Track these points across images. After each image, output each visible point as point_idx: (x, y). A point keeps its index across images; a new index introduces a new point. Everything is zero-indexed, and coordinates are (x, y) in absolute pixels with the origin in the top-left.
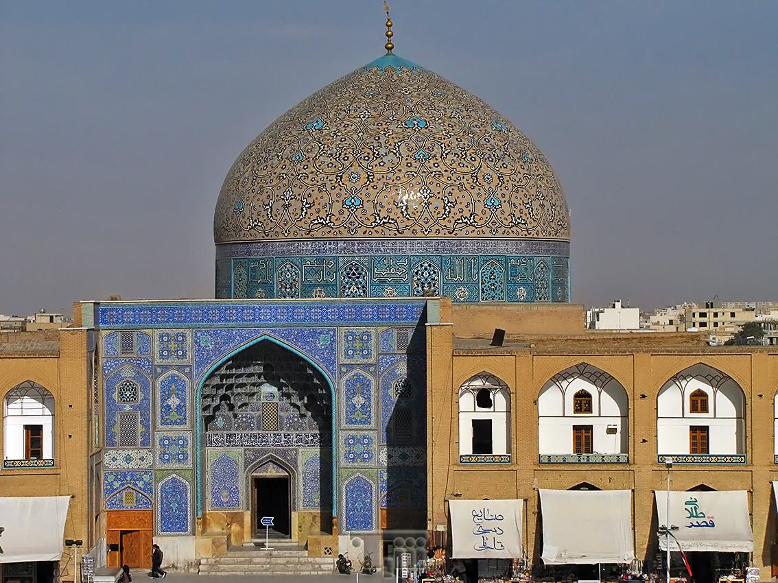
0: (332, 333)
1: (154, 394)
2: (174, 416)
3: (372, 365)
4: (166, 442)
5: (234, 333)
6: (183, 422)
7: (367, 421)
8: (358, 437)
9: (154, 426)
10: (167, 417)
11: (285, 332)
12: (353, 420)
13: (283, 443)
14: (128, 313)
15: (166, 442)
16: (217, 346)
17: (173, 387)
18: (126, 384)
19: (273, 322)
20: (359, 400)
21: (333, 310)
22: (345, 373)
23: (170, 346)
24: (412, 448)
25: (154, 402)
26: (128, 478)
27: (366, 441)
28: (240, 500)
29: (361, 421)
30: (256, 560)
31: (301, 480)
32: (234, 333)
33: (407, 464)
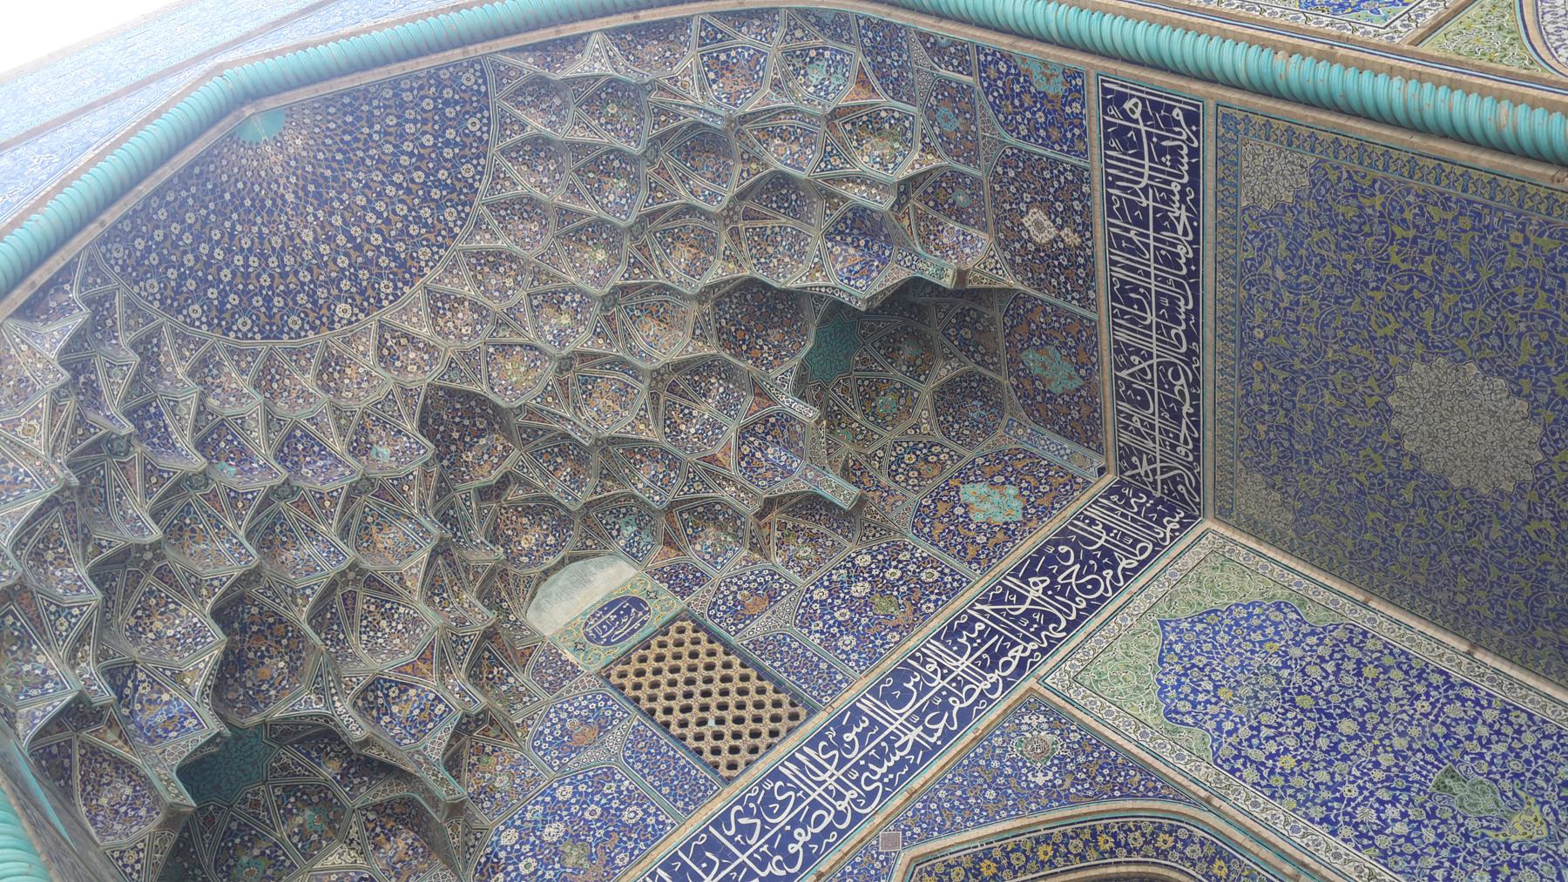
13: (912, 736)
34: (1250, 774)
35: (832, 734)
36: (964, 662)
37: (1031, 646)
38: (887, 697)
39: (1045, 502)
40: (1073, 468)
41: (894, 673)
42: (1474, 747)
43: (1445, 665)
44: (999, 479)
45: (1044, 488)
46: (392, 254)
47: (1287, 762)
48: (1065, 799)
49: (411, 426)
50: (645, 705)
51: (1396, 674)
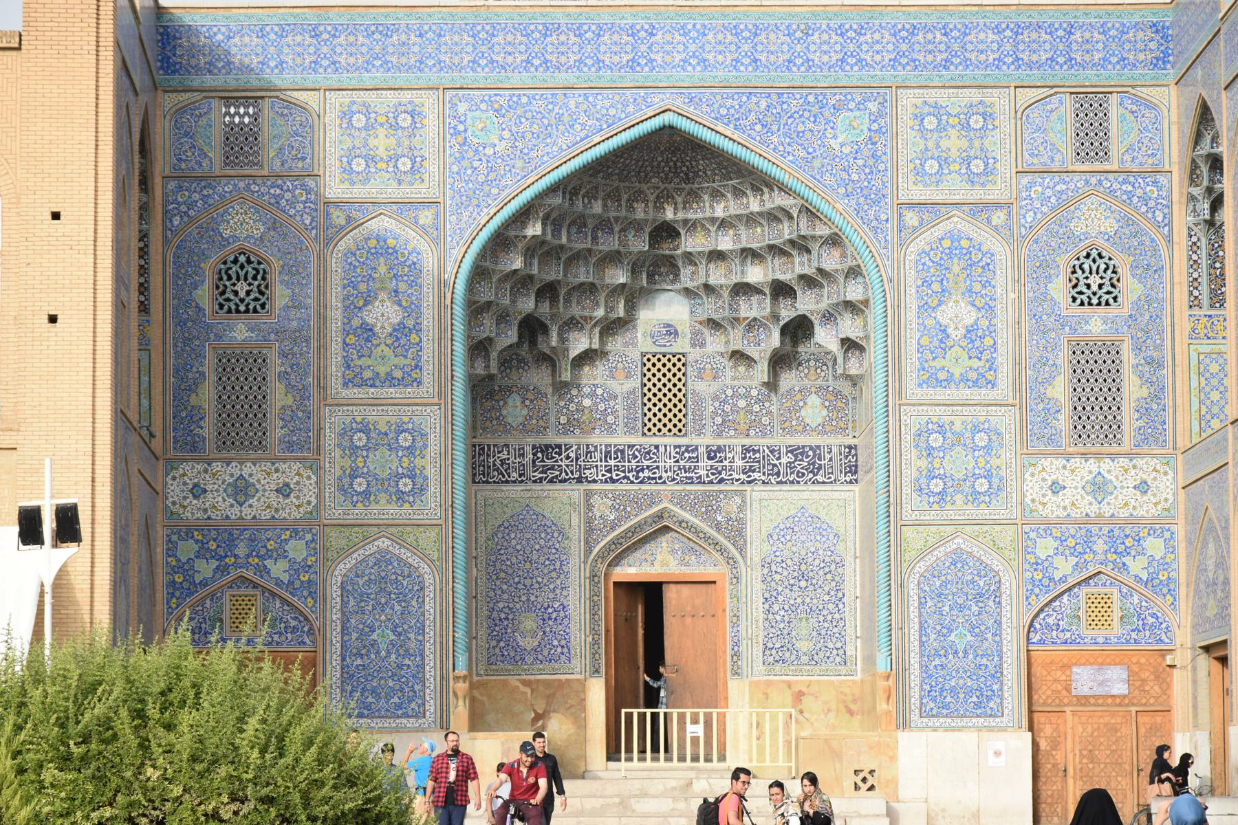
0: (873, 107)
1: (321, 291)
2: (384, 359)
3: (998, 205)
4: (360, 439)
5: (572, 104)
6: (410, 378)
7: (984, 380)
8: (958, 427)
9: (322, 388)
10: (364, 362)
11: (729, 102)
12: (942, 375)
13: (702, 472)
14: (247, 39)
15: (360, 439)
16: (519, 145)
17: (382, 269)
18: (235, 261)
19: (694, 74)
20: (958, 314)
21: (877, 36)
22: (915, 229)
23: (372, 142)
24: (1124, 462)
25: (322, 319)
26: (242, 550)
27: (981, 439)
28: (574, 643)
29: (964, 379)
30: (641, 806)
31: (759, 586)
32: (572, 104)
33: (1107, 510)
34: (766, 571)
35: (683, 449)
36: (739, 463)
37: (763, 478)
38: (709, 453)
39: (828, 428)
40: (850, 425)
41: (719, 447)
42: (821, 618)
43: (847, 594)
44: (827, 404)
45: (834, 423)
46: (687, 174)
47: (777, 577)
48: (718, 529)
49: (648, 230)
50: (645, 380)
51: (833, 584)
